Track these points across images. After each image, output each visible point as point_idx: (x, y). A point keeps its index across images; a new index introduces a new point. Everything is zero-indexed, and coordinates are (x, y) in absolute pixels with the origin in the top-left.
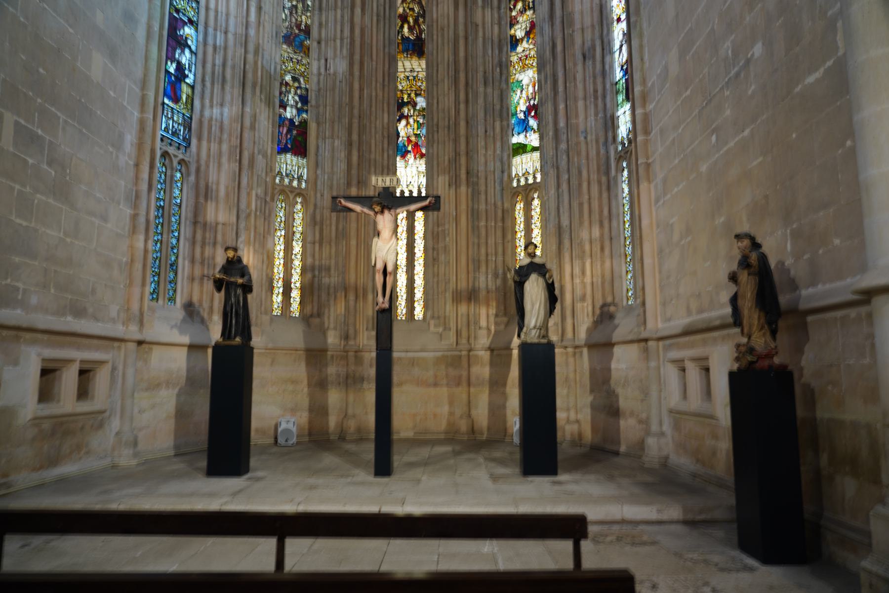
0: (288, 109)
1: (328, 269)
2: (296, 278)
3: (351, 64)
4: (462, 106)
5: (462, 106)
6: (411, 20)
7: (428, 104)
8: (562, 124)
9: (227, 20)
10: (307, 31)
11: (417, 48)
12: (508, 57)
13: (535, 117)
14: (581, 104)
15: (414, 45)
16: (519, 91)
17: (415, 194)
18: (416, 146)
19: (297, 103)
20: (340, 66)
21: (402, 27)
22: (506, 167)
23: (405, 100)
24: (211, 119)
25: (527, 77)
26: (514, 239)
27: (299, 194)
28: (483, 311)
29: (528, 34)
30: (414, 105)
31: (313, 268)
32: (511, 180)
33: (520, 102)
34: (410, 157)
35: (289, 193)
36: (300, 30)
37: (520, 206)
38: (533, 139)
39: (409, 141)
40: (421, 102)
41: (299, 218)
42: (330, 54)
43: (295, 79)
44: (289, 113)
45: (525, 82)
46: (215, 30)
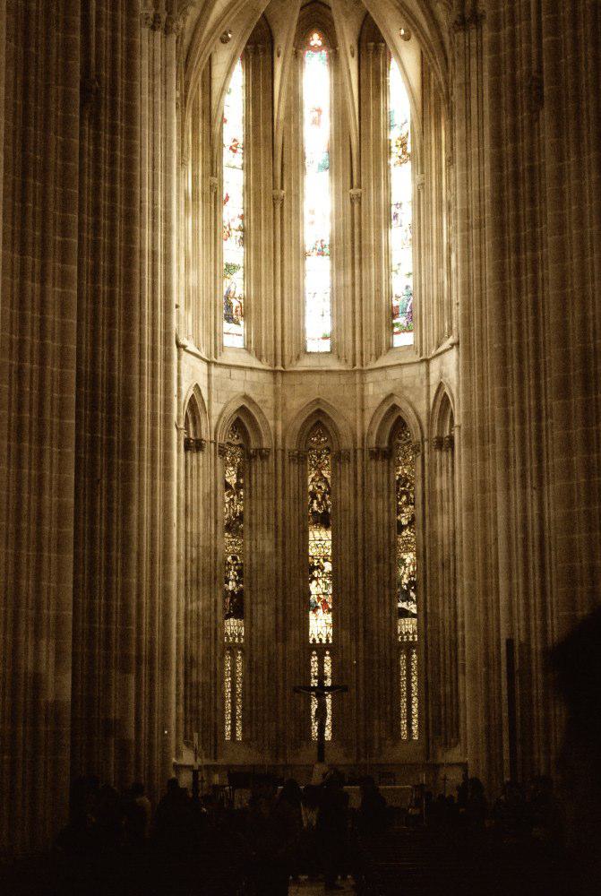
0: (230, 583)
4: (360, 580)
5: (360, 580)
6: (319, 496)
7: (333, 568)
8: (428, 610)
9: (198, 538)
11: (324, 521)
12: (396, 538)
13: (413, 590)
14: (440, 599)
15: (322, 518)
16: (403, 567)
17: (324, 642)
18: (325, 602)
19: (235, 576)
20: (267, 545)
21: (312, 502)
22: (393, 627)
23: (316, 564)
24: (192, 611)
25: (409, 557)
26: (399, 681)
27: (240, 649)
29: (411, 522)
32: (397, 635)
33: (405, 574)
34: (320, 611)
35: (232, 648)
36: (236, 518)
37: (403, 657)
38: (413, 608)
39: (319, 599)
40: (328, 567)
41: (239, 665)
43: (234, 558)
44: (231, 586)
45: (408, 561)
46: (192, 546)
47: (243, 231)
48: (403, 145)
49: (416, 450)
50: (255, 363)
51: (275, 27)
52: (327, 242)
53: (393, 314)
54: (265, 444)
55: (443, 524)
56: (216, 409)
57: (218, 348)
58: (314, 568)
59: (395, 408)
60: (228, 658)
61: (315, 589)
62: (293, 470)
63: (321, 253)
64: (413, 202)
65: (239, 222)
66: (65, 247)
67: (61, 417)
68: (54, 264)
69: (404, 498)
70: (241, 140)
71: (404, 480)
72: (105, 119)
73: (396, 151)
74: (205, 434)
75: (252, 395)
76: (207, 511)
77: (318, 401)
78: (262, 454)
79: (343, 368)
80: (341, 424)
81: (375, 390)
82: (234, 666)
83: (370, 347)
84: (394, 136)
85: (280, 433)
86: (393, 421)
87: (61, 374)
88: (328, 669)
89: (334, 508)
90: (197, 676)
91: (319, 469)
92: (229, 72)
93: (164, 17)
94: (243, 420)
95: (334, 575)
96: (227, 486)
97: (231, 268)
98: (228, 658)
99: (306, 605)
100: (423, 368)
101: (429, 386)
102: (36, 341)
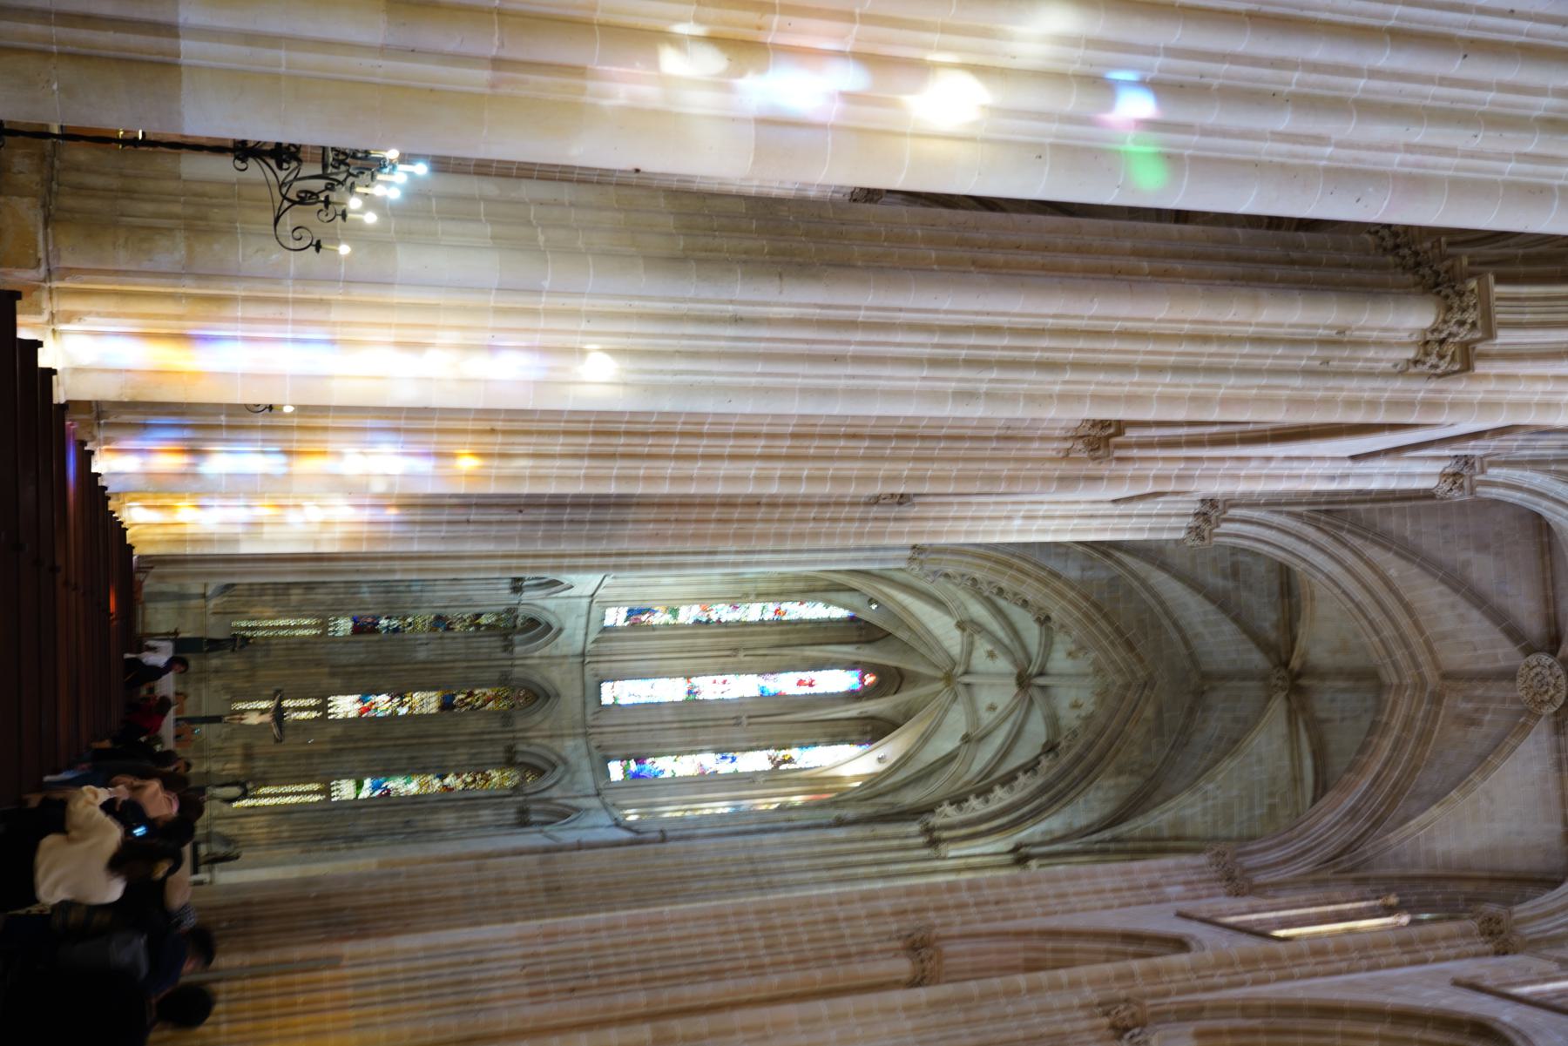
1: (267, 656)
2: (260, 633)
3: (424, 662)
10: (448, 629)
11: (446, 705)
18: (368, 709)
20: (422, 654)
22: (347, 776)
25: (413, 787)
28: (236, 765)
29: (447, 788)
30: (402, 704)
31: (268, 645)
34: (359, 706)
35: (324, 625)
37: (316, 787)
38: (365, 794)
40: (403, 711)
41: (306, 632)
42: (431, 646)
44: (384, 622)
47: (708, 622)
48: (784, 762)
49: (516, 789)
50: (591, 638)
51: (879, 644)
52: (700, 697)
53: (640, 760)
54: (518, 649)
55: (447, 819)
56: (550, 604)
57: (606, 604)
58: (402, 696)
59: (554, 766)
60: (314, 622)
61: (385, 697)
62: (494, 675)
63: (689, 692)
64: (736, 772)
65: (715, 618)
66: (796, 479)
67: (618, 478)
68: (779, 468)
69: (469, 780)
70: (785, 618)
71: (487, 779)
72: (875, 511)
73: (783, 752)
74: (527, 596)
75: (563, 635)
76: (455, 599)
77: (558, 695)
78: (508, 647)
79: (589, 718)
80: (537, 717)
81: (571, 748)
82: (306, 627)
83: (607, 740)
84: (794, 752)
85: (529, 662)
86: (544, 766)
87: (664, 478)
88: (304, 715)
89: (457, 715)
90: (296, 596)
91: (495, 698)
92: (845, 607)
93: (922, 557)
94: (537, 627)
95: (394, 716)
96: (478, 616)
97: (674, 612)
98: (314, 622)
99: (366, 692)
100: (592, 791)
101: (575, 797)
102: (700, 451)
